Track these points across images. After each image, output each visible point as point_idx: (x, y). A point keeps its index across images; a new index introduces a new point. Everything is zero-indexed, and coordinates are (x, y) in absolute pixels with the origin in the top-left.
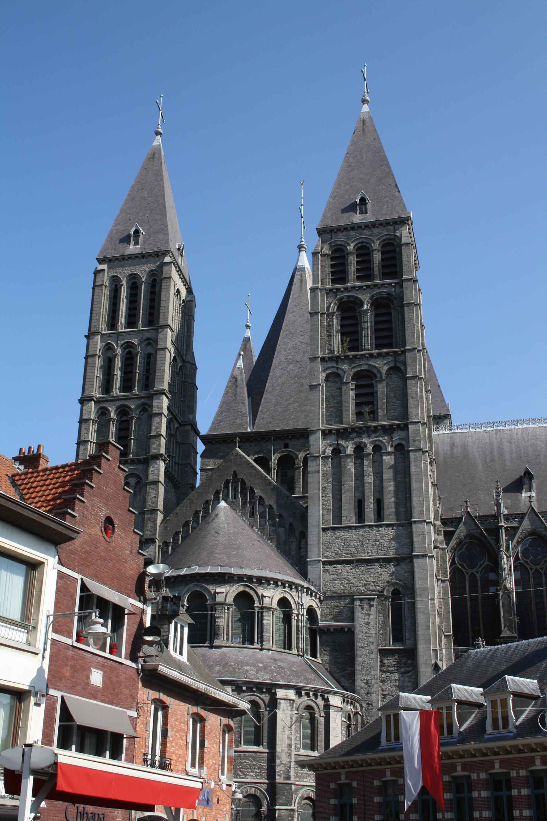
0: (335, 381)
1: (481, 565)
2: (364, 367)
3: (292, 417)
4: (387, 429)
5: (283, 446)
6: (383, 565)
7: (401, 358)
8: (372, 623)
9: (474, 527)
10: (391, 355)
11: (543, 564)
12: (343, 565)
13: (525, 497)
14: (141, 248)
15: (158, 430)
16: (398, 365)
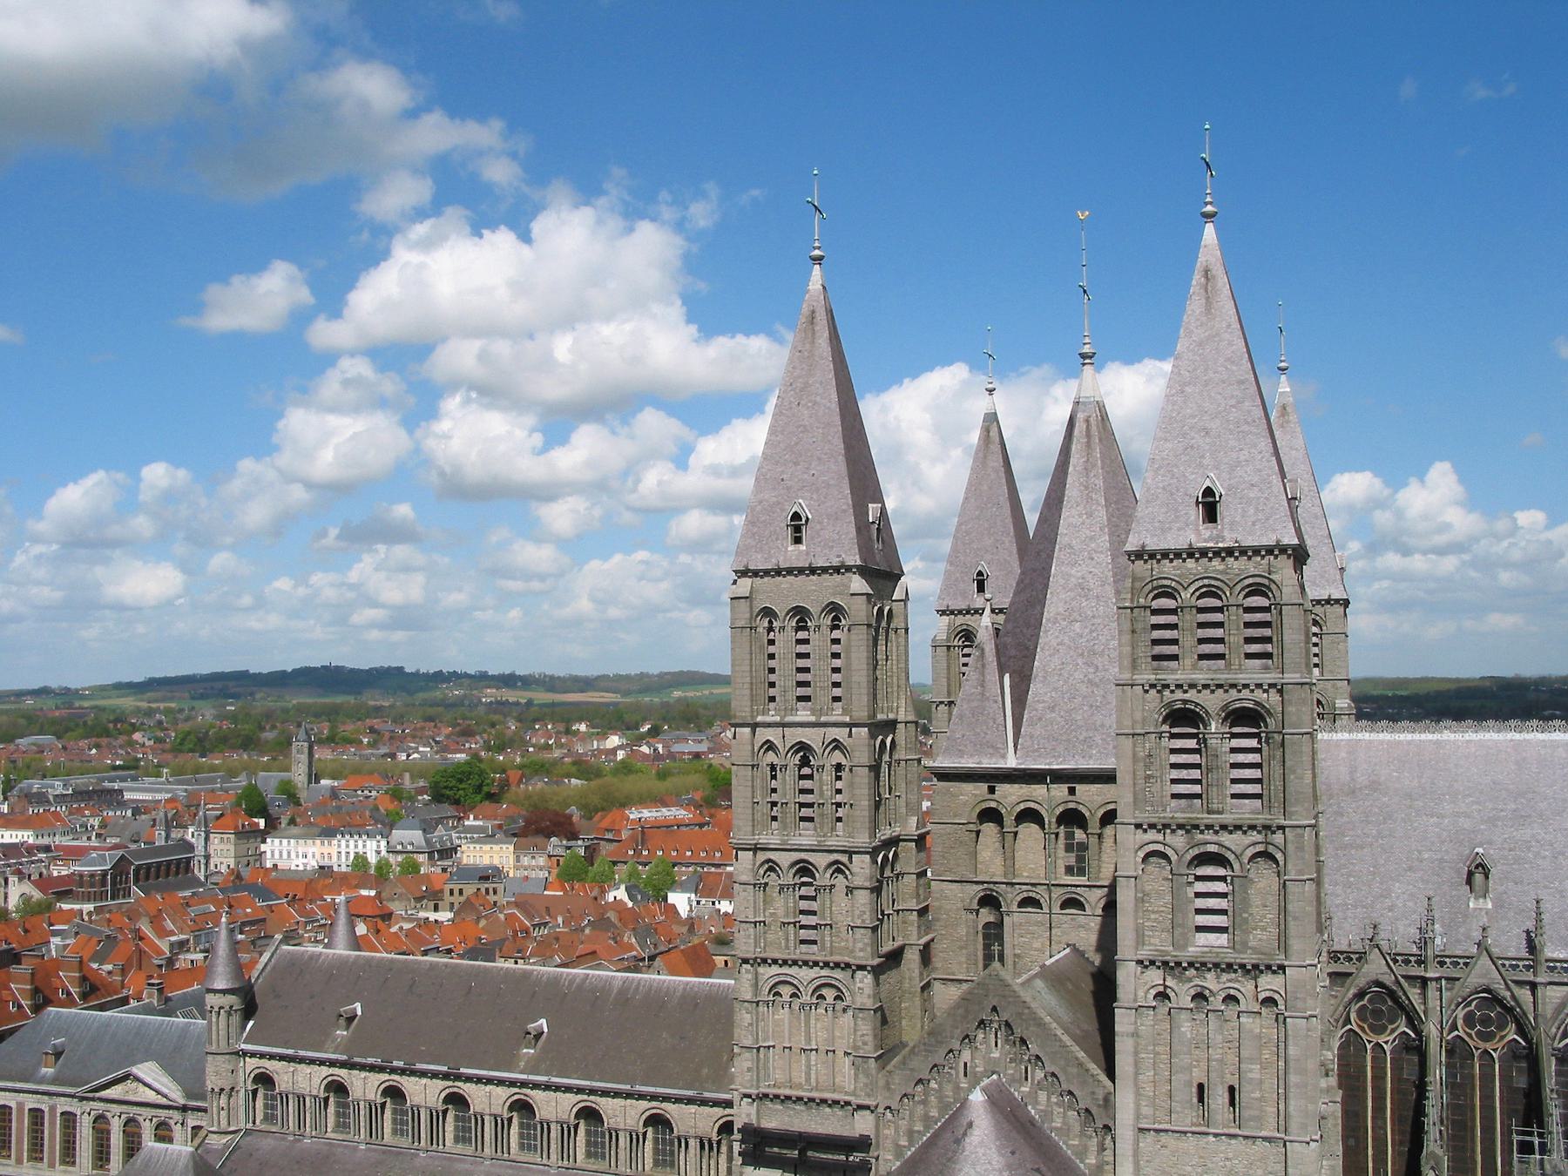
0: (1160, 864)
1: (1393, 1031)
2: (1212, 848)
3: (1081, 738)
7: (1278, 838)
9: (1386, 969)
10: (1259, 832)
11: (1499, 1041)
13: (1475, 909)
14: (808, 554)
15: (865, 917)
16: (1271, 849)
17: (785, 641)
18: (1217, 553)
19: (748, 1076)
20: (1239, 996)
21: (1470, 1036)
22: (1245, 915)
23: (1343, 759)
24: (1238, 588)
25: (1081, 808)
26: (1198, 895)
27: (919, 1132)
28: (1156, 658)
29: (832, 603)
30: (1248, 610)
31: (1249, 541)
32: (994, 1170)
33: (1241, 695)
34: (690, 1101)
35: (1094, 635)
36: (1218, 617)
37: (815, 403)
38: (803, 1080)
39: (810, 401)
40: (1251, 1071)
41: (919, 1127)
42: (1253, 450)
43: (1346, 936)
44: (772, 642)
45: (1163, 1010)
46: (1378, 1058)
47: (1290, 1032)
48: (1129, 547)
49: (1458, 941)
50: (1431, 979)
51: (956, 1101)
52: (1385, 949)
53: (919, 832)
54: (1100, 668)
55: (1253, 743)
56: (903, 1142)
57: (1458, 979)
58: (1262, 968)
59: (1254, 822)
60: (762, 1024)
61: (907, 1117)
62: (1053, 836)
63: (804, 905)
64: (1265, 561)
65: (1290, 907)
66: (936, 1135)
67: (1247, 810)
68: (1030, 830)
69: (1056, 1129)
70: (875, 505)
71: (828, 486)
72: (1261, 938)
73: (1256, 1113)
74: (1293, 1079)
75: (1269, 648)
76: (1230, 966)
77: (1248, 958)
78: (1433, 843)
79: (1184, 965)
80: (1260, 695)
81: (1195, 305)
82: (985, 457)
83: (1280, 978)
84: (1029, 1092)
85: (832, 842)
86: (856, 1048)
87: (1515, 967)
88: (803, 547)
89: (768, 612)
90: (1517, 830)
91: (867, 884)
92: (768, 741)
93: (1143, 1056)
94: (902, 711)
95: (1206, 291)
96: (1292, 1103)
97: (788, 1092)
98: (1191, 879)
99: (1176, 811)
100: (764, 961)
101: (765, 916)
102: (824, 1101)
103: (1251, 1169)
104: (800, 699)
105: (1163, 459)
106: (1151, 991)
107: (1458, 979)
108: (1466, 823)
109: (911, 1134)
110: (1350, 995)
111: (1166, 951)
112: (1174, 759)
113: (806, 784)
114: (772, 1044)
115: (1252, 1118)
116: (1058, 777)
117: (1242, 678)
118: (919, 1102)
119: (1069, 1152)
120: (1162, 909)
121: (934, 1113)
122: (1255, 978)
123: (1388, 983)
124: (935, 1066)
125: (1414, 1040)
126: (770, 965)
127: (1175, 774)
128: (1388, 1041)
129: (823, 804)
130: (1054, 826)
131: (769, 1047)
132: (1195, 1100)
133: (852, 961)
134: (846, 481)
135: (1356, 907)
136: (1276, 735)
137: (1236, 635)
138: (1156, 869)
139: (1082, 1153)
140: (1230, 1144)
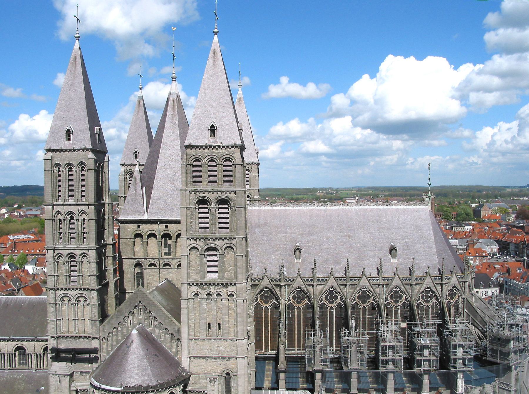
1: (271, 302)
2: (212, 245)
3: (170, 209)
4: (225, 285)
5: (165, 228)
6: (222, 360)
7: (234, 241)
8: (216, 390)
10: (228, 240)
12: (200, 359)
14: (72, 144)
15: (94, 272)
16: (232, 245)
17: (64, 176)
18: (215, 147)
19: (53, 330)
20: (222, 294)
21: (294, 302)
22: (223, 267)
23: (256, 215)
24: (222, 159)
25: (169, 233)
26: (208, 261)
27: (115, 345)
28: (194, 182)
29: (82, 162)
30: (225, 166)
31: (226, 143)
32: (141, 356)
33: (222, 195)
34: (32, 340)
35: (174, 174)
36: (215, 168)
37: (76, 90)
38: (73, 330)
39: (74, 89)
40: (226, 318)
41: (115, 343)
42: (228, 113)
43: (256, 272)
44: (59, 176)
45: (197, 299)
46: (266, 311)
47: (238, 305)
48: (185, 144)
49: (291, 273)
50: (283, 285)
51: (127, 334)
52: (269, 276)
53: (113, 242)
54: (176, 185)
55: (226, 210)
56: (110, 349)
57: (291, 285)
58: (229, 284)
59: (226, 237)
60: (57, 311)
61: (111, 341)
62: (160, 242)
63: (72, 269)
64: (231, 150)
65: (238, 264)
66: (120, 346)
67: (223, 233)
68: (152, 240)
69: (162, 341)
70: (97, 127)
71: (80, 120)
72: (228, 275)
73: (228, 331)
74: (239, 319)
75: (231, 179)
76: (218, 284)
77: (224, 281)
78: (283, 242)
79: (204, 284)
80: (228, 195)
81: (210, 62)
82: (138, 111)
83: (234, 288)
84: (153, 329)
85: (82, 246)
86: (92, 318)
87: (307, 280)
88: (71, 142)
89: (58, 165)
90: (309, 237)
91: (95, 261)
92: (58, 211)
93: (190, 315)
94: (107, 200)
95: (214, 58)
96: (239, 327)
97: (68, 335)
98: (206, 256)
99: (201, 233)
100: (58, 289)
101: (58, 273)
102: (81, 337)
103: (226, 349)
104: (70, 196)
105: (198, 115)
106: (193, 293)
107: (291, 285)
108: (294, 235)
109: (112, 346)
110: (258, 292)
111: (197, 280)
112: (200, 216)
113: (72, 226)
114: (61, 318)
115: (226, 333)
116: (162, 222)
117: (223, 189)
118: (115, 335)
119: (166, 348)
120: (197, 266)
121: (120, 338)
122: (227, 288)
123: (269, 287)
124: (120, 322)
125: (277, 305)
126: (60, 290)
127: (200, 221)
128: (269, 306)
129: (79, 233)
130: (160, 239)
131: (60, 319)
132: (208, 328)
133: (90, 288)
134: (87, 119)
135: (259, 263)
136: (233, 208)
137: (204, 176)
138: (194, 253)
139: (171, 348)
140: (219, 342)
